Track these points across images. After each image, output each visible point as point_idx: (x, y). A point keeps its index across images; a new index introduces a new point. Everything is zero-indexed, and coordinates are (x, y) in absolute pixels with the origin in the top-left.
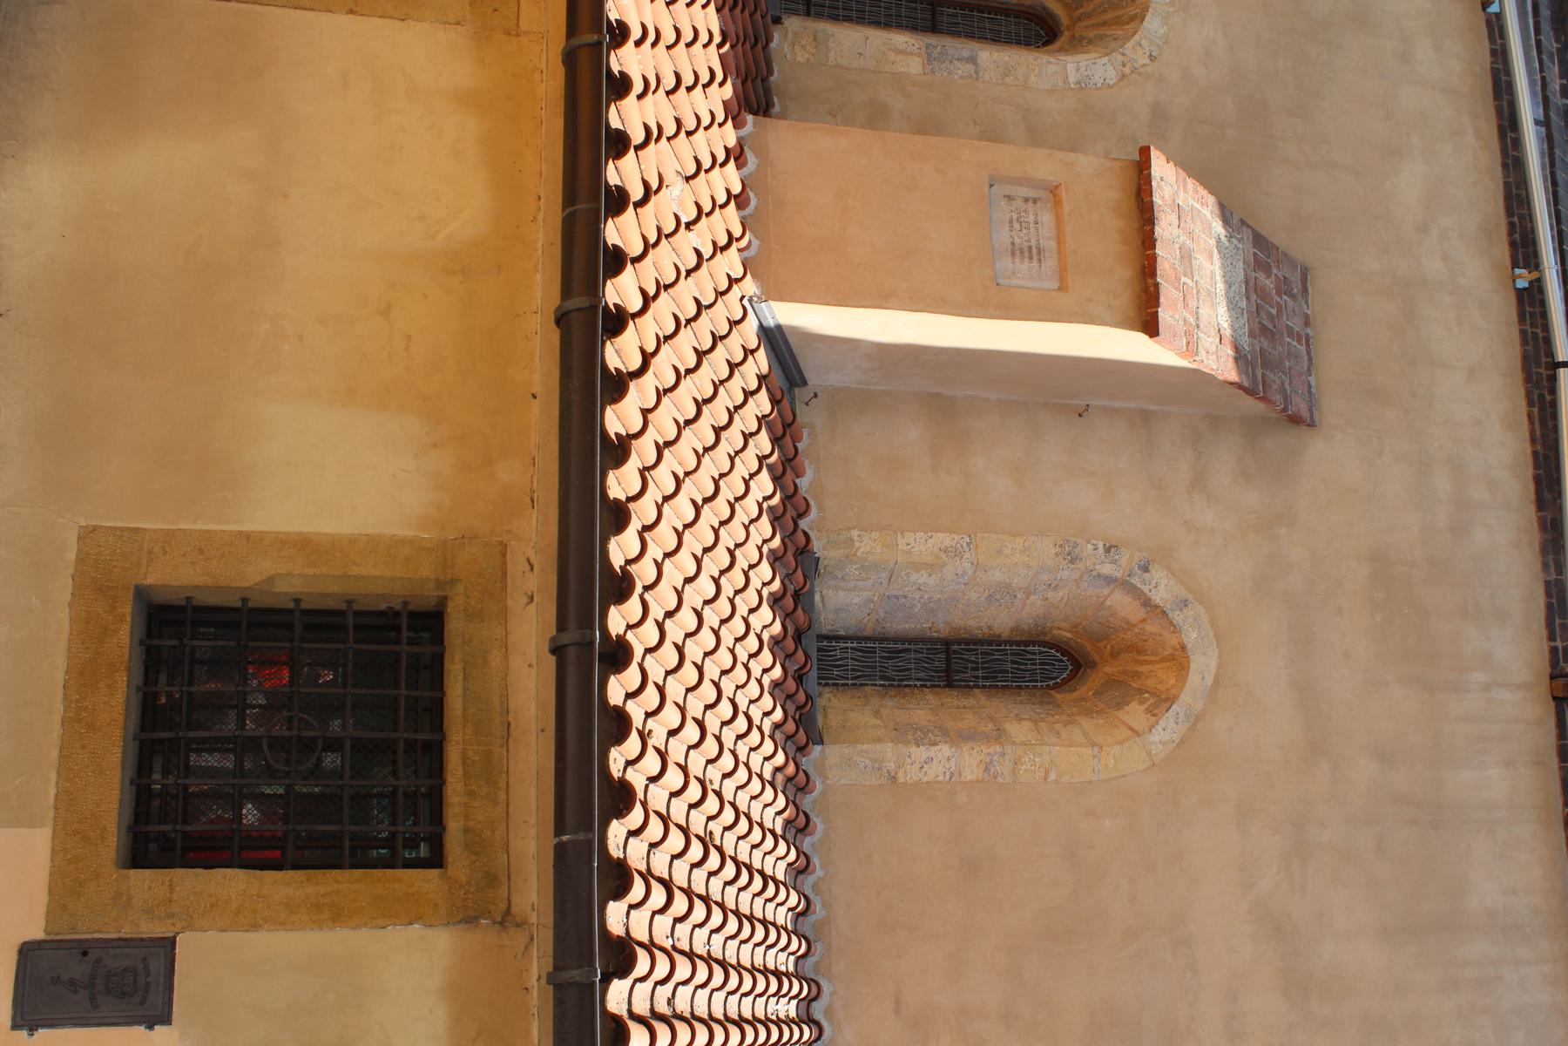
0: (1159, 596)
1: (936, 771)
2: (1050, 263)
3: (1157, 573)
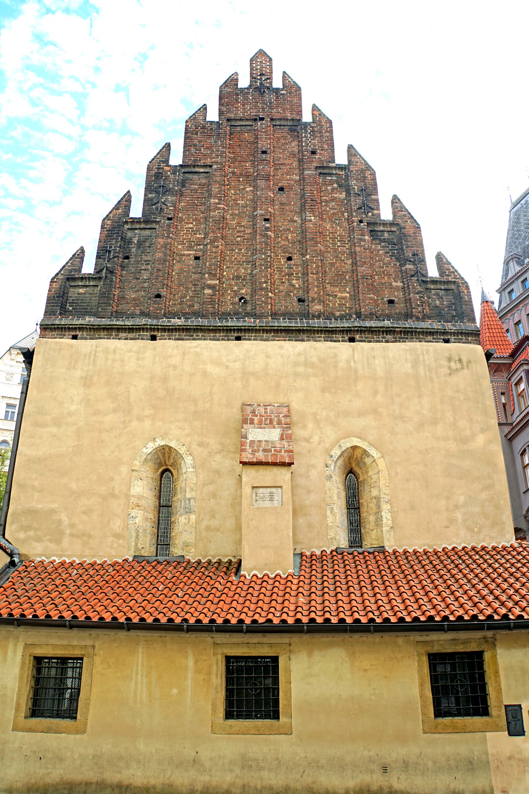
0: (339, 453)
1: (389, 516)
3: (333, 453)
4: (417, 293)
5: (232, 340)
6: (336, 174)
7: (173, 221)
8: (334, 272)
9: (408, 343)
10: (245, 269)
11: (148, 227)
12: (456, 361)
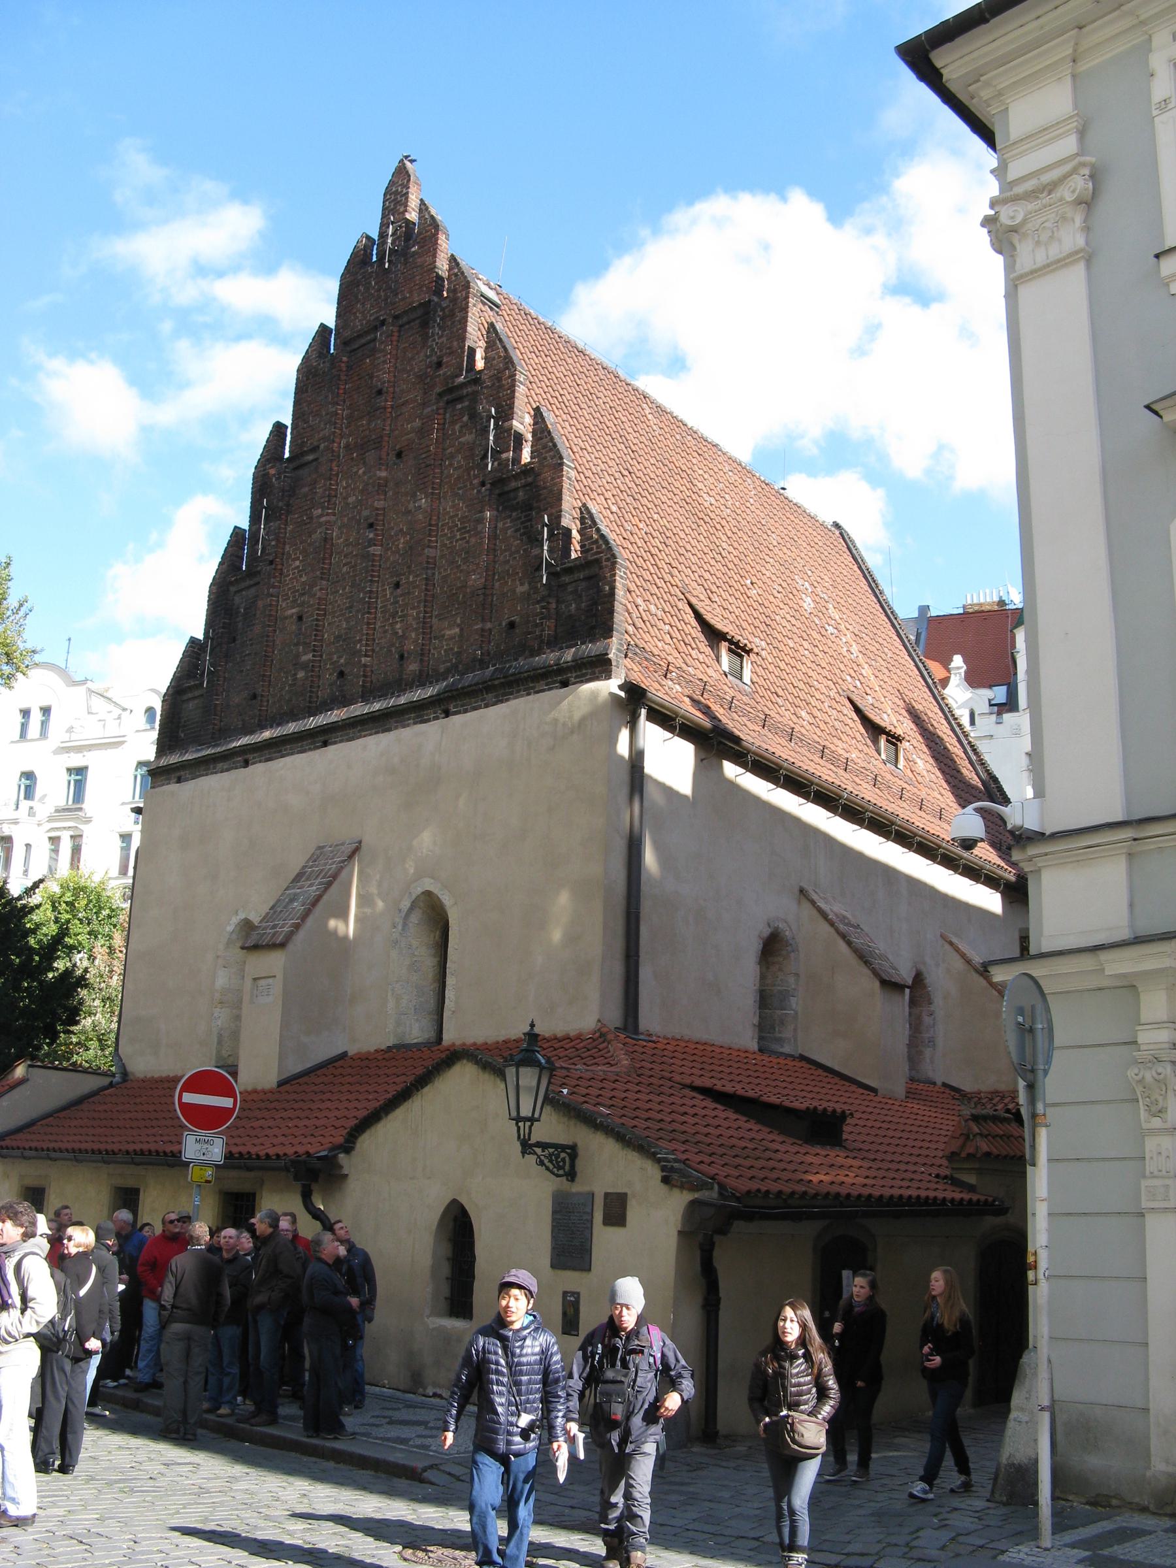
2: (271, 980)
4: (538, 602)
5: (318, 748)
6: (467, 395)
7: (273, 566)
10: (348, 622)
11: (252, 582)
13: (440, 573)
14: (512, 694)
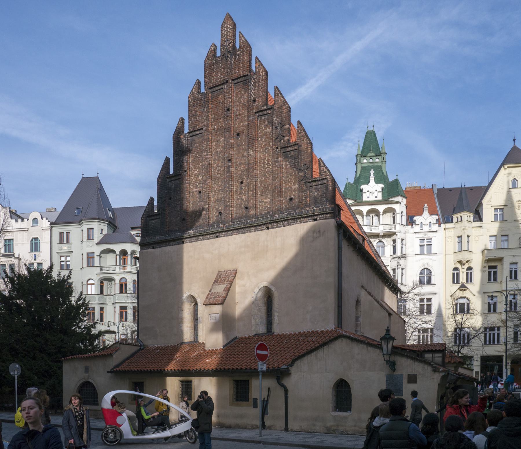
3: (255, 291)
8: (263, 186)
9: (295, 225)
12: (317, 232)
13: (260, 179)
14: (294, 222)
